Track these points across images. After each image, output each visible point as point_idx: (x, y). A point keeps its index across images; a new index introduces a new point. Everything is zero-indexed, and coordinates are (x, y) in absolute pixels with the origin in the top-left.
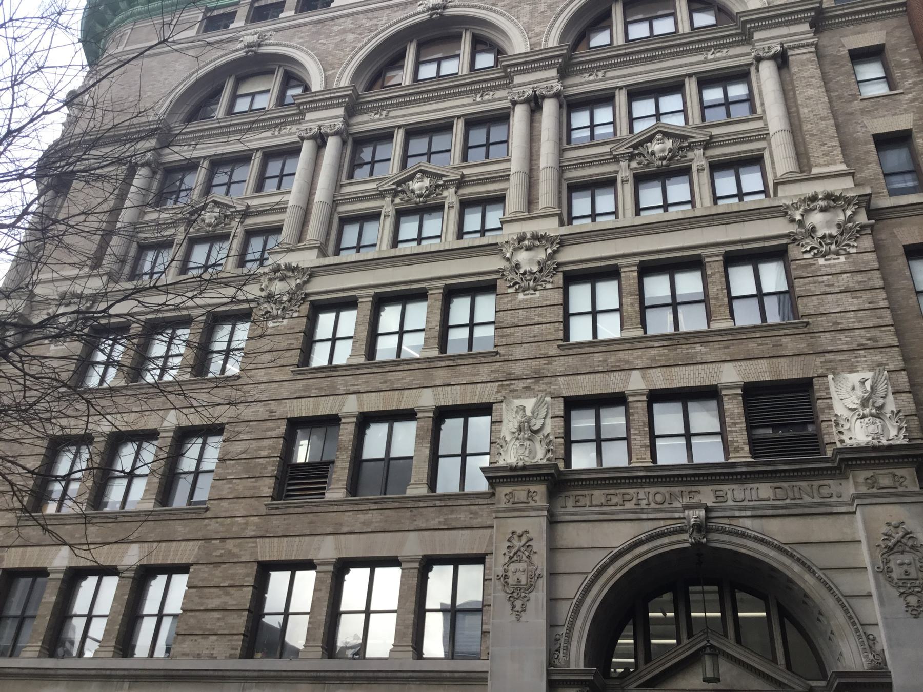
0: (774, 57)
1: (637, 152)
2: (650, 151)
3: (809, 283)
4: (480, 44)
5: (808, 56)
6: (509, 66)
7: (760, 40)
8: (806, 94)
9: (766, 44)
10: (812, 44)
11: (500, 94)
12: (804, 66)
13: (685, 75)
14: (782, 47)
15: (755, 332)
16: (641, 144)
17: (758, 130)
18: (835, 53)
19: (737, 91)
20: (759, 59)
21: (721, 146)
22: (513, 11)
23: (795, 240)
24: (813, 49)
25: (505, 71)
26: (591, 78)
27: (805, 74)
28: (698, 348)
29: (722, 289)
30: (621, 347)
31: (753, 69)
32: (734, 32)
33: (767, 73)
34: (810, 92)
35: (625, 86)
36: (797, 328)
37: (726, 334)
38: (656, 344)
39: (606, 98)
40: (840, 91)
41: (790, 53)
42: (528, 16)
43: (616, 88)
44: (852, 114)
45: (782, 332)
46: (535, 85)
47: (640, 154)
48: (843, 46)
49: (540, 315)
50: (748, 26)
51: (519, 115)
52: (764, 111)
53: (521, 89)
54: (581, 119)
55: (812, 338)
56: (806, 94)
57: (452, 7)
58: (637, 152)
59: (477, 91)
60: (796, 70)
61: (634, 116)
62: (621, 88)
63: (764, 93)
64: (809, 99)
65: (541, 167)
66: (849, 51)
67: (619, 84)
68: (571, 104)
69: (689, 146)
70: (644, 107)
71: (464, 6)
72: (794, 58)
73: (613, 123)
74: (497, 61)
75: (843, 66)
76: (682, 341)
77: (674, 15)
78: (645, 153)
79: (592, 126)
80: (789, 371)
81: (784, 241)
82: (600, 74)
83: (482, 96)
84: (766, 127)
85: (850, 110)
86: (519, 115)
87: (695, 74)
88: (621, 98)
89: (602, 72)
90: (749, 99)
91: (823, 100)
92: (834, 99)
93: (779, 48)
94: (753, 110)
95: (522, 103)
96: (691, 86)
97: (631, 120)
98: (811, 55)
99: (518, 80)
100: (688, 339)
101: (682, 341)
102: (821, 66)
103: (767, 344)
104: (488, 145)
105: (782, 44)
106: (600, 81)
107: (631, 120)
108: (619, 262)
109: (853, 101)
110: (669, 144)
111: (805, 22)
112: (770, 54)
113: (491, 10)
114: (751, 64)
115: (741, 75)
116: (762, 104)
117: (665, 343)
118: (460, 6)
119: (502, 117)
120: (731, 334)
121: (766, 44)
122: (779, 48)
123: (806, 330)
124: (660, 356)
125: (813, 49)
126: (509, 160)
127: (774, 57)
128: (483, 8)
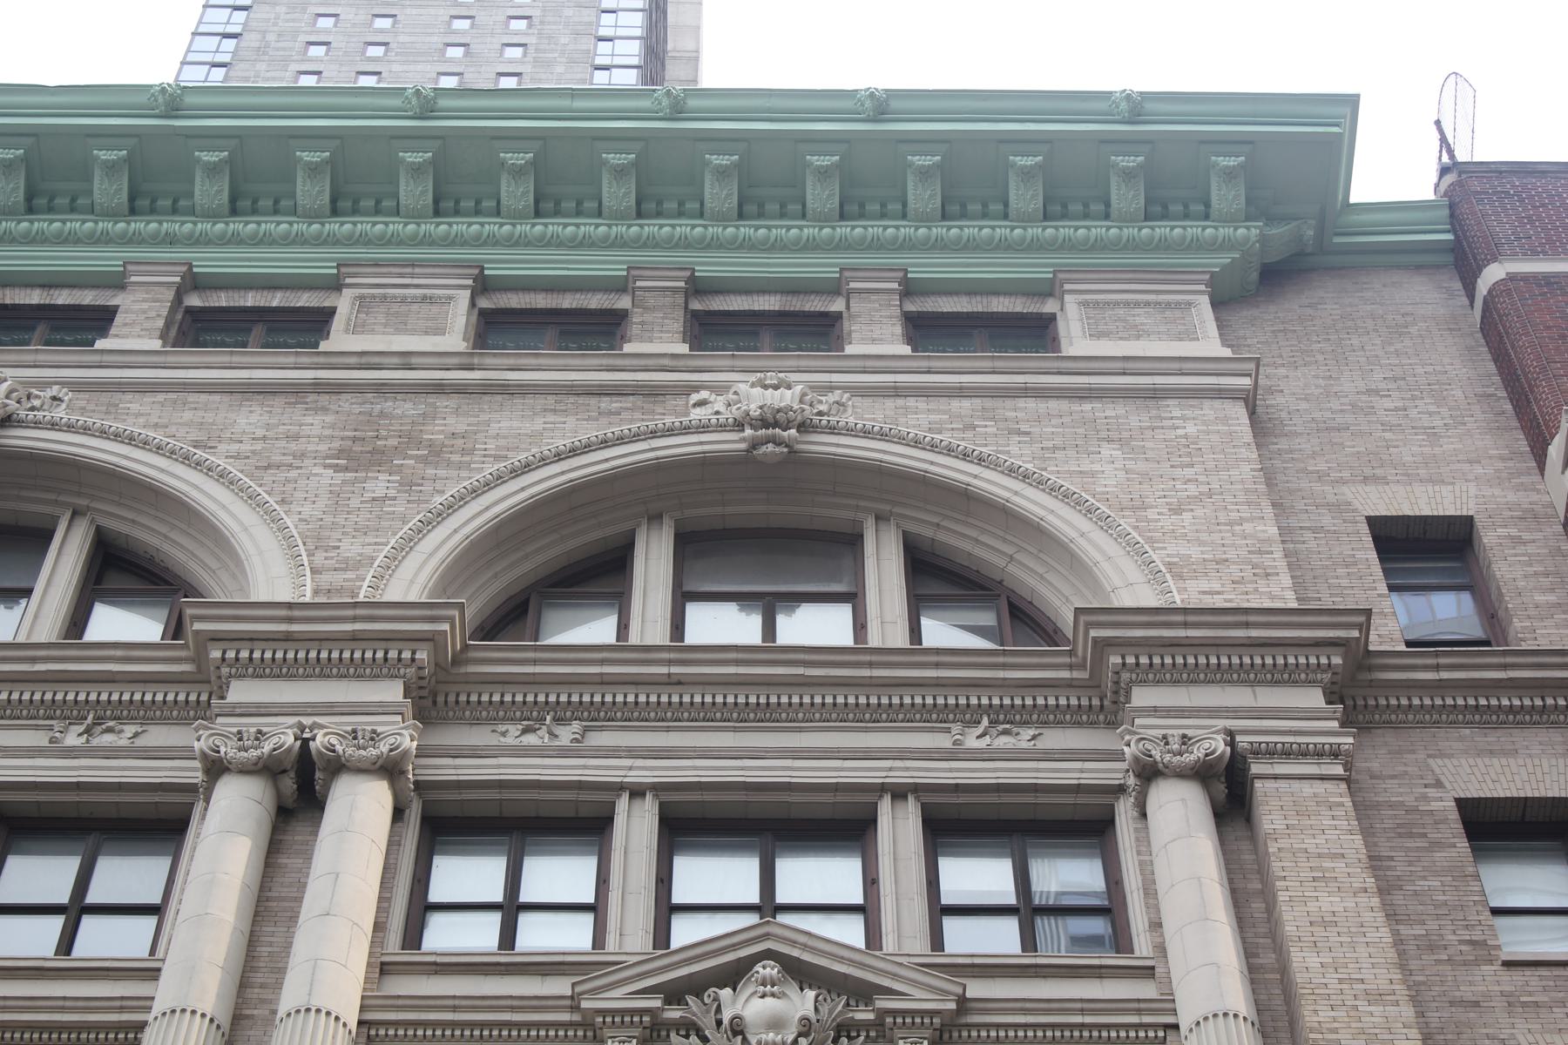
0: (1202, 773)
1: (674, 1014)
2: (726, 1016)
4: (118, 570)
5: (1320, 787)
6: (216, 638)
7: (1155, 711)
8: (1312, 906)
9: (1175, 728)
10: (1335, 753)
11: (158, 736)
12: (1305, 819)
13: (882, 789)
14: (1232, 743)
16: (697, 986)
17: (1138, 1006)
18: (1409, 800)
19: (1067, 875)
20: (1149, 773)
22: (268, 477)
24: (1339, 770)
25: (199, 658)
26: (530, 739)
27: (1309, 844)
31: (1124, 811)
32: (1065, 674)
33: (1178, 824)
34: (1328, 902)
35: (657, 788)
39: (580, 822)
40: (1432, 925)
41: (1255, 769)
42: (321, 504)
43: (619, 788)
44: (1476, 1004)
48: (1439, 784)
50: (1115, 660)
51: (229, 829)
52: (1161, 949)
53: (251, 724)
54: (468, 875)
56: (1312, 906)
57: (37, 425)
58: (674, 1014)
59: (71, 713)
60: (1279, 824)
61: (677, 898)
62: (637, 792)
63: (1161, 886)
64: (1325, 924)
65: (281, 1013)
66: (1461, 803)
67: (634, 777)
68: (444, 820)
69: (878, 1024)
70: (718, 877)
71: (86, 430)
72: (1270, 784)
73: (596, 909)
74: (176, 629)
75: (1437, 845)
77: (854, 598)
78: (707, 1024)
79: (511, 909)
82: (566, 734)
83: (88, 731)
84: (1167, 1003)
85: (1466, 992)
86: (229, 829)
87: (917, 789)
88: (636, 828)
89: (576, 726)
90: (1111, 908)
91: (1372, 936)
92: (1411, 948)
93: (1220, 746)
94: (1121, 940)
95: (246, 770)
96: (899, 831)
97: (666, 909)
98: (1330, 786)
99: (240, 692)
102: (1367, 833)
104: (76, 910)
105: (1231, 734)
106: (563, 753)
107: (666, 909)
109: (1477, 962)
110: (802, 1003)
111: (1310, 683)
112: (1189, 758)
113: (186, 459)
114: (1121, 789)
115: (1085, 824)
116: (1156, 925)
118: (70, 428)
119: (159, 824)
121: (1175, 728)
122: (1220, 746)
125: (1339, 770)
126: (153, 974)
127: (1202, 773)
128: (158, 449)
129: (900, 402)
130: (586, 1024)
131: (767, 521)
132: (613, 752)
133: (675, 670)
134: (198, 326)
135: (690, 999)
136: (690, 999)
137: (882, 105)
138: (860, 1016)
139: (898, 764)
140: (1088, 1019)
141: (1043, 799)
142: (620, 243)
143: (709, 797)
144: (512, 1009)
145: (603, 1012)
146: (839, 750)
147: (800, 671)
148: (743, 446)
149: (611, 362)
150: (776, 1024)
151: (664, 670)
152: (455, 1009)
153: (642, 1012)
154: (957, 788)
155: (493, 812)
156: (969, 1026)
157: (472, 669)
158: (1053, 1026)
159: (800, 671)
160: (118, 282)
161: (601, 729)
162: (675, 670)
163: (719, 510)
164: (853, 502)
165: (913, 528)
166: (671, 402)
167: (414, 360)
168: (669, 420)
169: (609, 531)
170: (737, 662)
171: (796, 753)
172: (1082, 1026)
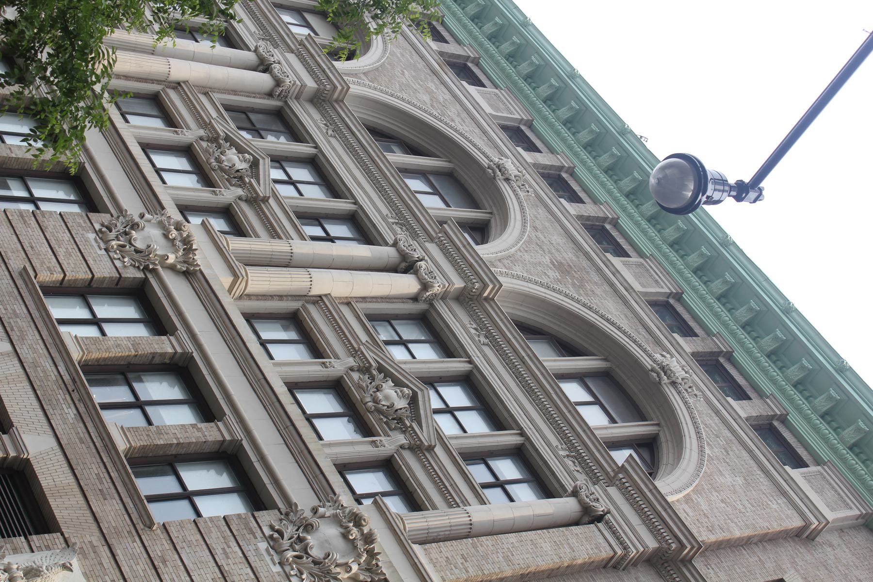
1: (374, 372)
3: (222, 532)
15: (118, 471)
20: (575, 493)
21: (424, 467)
23: (287, 514)
26: (473, 331)
28: (71, 413)
29: (177, 438)
30: (45, 333)
32: (609, 470)
36: (140, 516)
37: (102, 440)
38: (62, 368)
45: (127, 500)
46: (426, 258)
47: (372, 378)
49: (68, 254)
55: (129, 532)
76: (75, 395)
80: (64, 505)
81: (280, 504)
100: (81, 399)
101: (75, 395)
103: (102, 483)
108: (181, 331)
110: (401, 404)
117: (66, 377)
120: (106, 446)
123: (140, 526)
124: (44, 371)
129: (713, 414)
130: (356, 352)
131: (626, 385)
132: (485, 356)
133: (526, 358)
134: (768, 430)
135: (383, 375)
136: (383, 375)
137: (789, 309)
138: (407, 422)
139: (534, 431)
140: (449, 488)
141: (500, 407)
142: (726, 325)
143: (483, 382)
144: (350, 332)
145: (362, 353)
146: (527, 412)
147: (552, 392)
148: (650, 368)
149: (720, 397)
150: (387, 398)
151: (524, 354)
152: (340, 318)
153: (369, 362)
154: (537, 450)
155: (438, 330)
156: (424, 455)
157: (487, 305)
158: (440, 479)
159: (552, 392)
160: (761, 395)
161: (491, 349)
162: (526, 358)
163: (625, 378)
164: (658, 414)
165: (661, 435)
166: (659, 349)
167: (618, 275)
168: (648, 348)
169: (590, 348)
170: (542, 374)
171: (340, 157)
172: (446, 487)
